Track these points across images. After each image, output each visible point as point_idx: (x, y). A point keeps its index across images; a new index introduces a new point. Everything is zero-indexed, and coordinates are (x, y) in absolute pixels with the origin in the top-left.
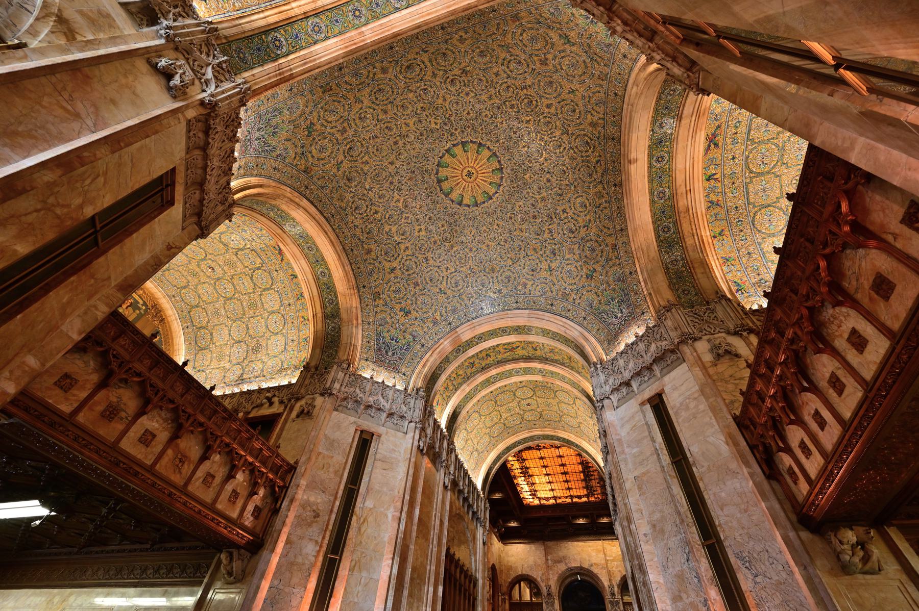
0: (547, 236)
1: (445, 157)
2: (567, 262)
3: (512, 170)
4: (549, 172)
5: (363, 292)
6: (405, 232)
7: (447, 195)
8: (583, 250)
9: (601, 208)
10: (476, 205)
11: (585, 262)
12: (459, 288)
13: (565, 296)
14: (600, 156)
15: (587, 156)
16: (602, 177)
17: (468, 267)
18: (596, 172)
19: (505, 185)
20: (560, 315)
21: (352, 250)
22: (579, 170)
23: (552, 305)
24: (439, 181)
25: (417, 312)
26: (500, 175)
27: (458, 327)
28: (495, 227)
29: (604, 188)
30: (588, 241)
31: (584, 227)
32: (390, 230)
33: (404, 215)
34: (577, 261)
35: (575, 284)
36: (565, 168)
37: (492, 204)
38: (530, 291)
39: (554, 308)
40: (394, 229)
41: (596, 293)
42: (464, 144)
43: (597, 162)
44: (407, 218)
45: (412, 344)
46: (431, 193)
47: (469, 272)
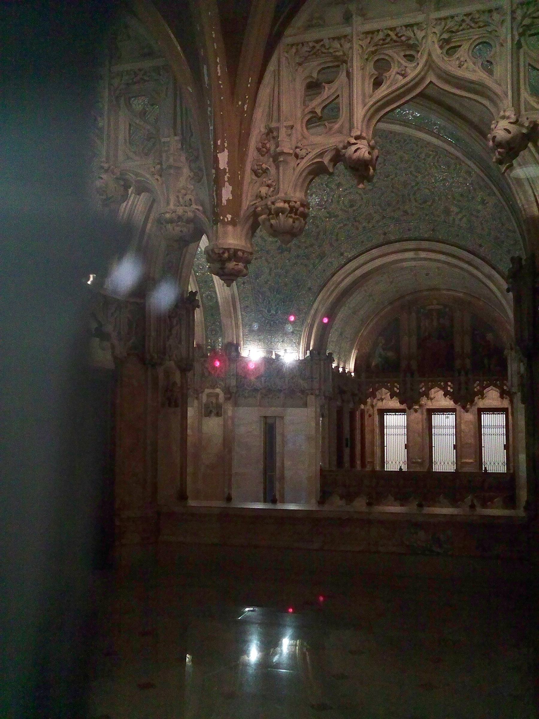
4: (385, 160)
9: (355, 224)
14: (413, 215)
15: (410, 200)
16: (390, 218)
18: (394, 211)
22: (392, 192)
29: (378, 222)
43: (406, 212)
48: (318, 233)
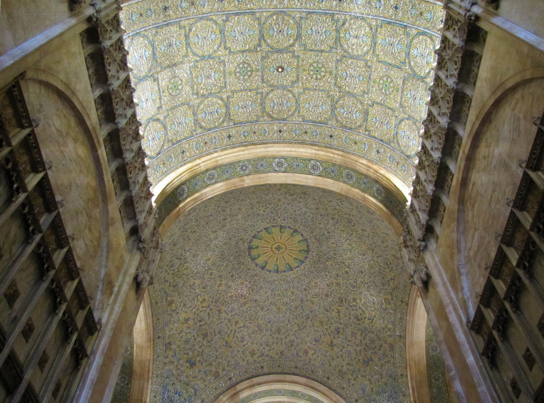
0: (334, 314)
1: (262, 232)
2: (349, 343)
3: (318, 255)
4: (349, 267)
5: (157, 343)
6: (206, 286)
7: (253, 259)
8: (364, 338)
10: (277, 271)
11: (364, 349)
12: (245, 343)
13: (341, 374)
17: (256, 324)
18: (389, 285)
19: (307, 263)
20: (334, 391)
21: (157, 303)
23: (328, 378)
24: (250, 248)
25: (202, 364)
26: (305, 255)
27: (237, 383)
28: (289, 293)
30: (370, 332)
31: (369, 319)
32: (194, 283)
33: (210, 271)
34: (357, 345)
35: (352, 365)
36: (363, 270)
37: (291, 275)
38: (310, 359)
39: (330, 382)
40: (197, 282)
41: (370, 380)
42: (281, 227)
43: (392, 279)
44: (211, 274)
45: (193, 399)
46: (239, 256)
47: (256, 329)
48: (377, 335)
